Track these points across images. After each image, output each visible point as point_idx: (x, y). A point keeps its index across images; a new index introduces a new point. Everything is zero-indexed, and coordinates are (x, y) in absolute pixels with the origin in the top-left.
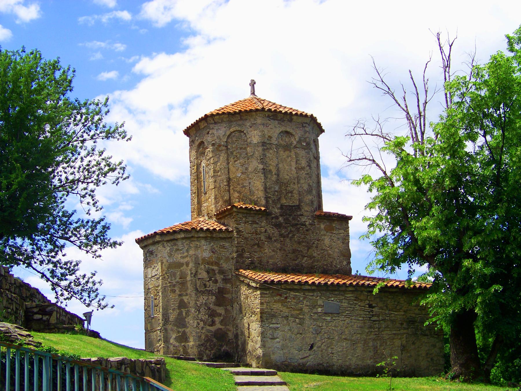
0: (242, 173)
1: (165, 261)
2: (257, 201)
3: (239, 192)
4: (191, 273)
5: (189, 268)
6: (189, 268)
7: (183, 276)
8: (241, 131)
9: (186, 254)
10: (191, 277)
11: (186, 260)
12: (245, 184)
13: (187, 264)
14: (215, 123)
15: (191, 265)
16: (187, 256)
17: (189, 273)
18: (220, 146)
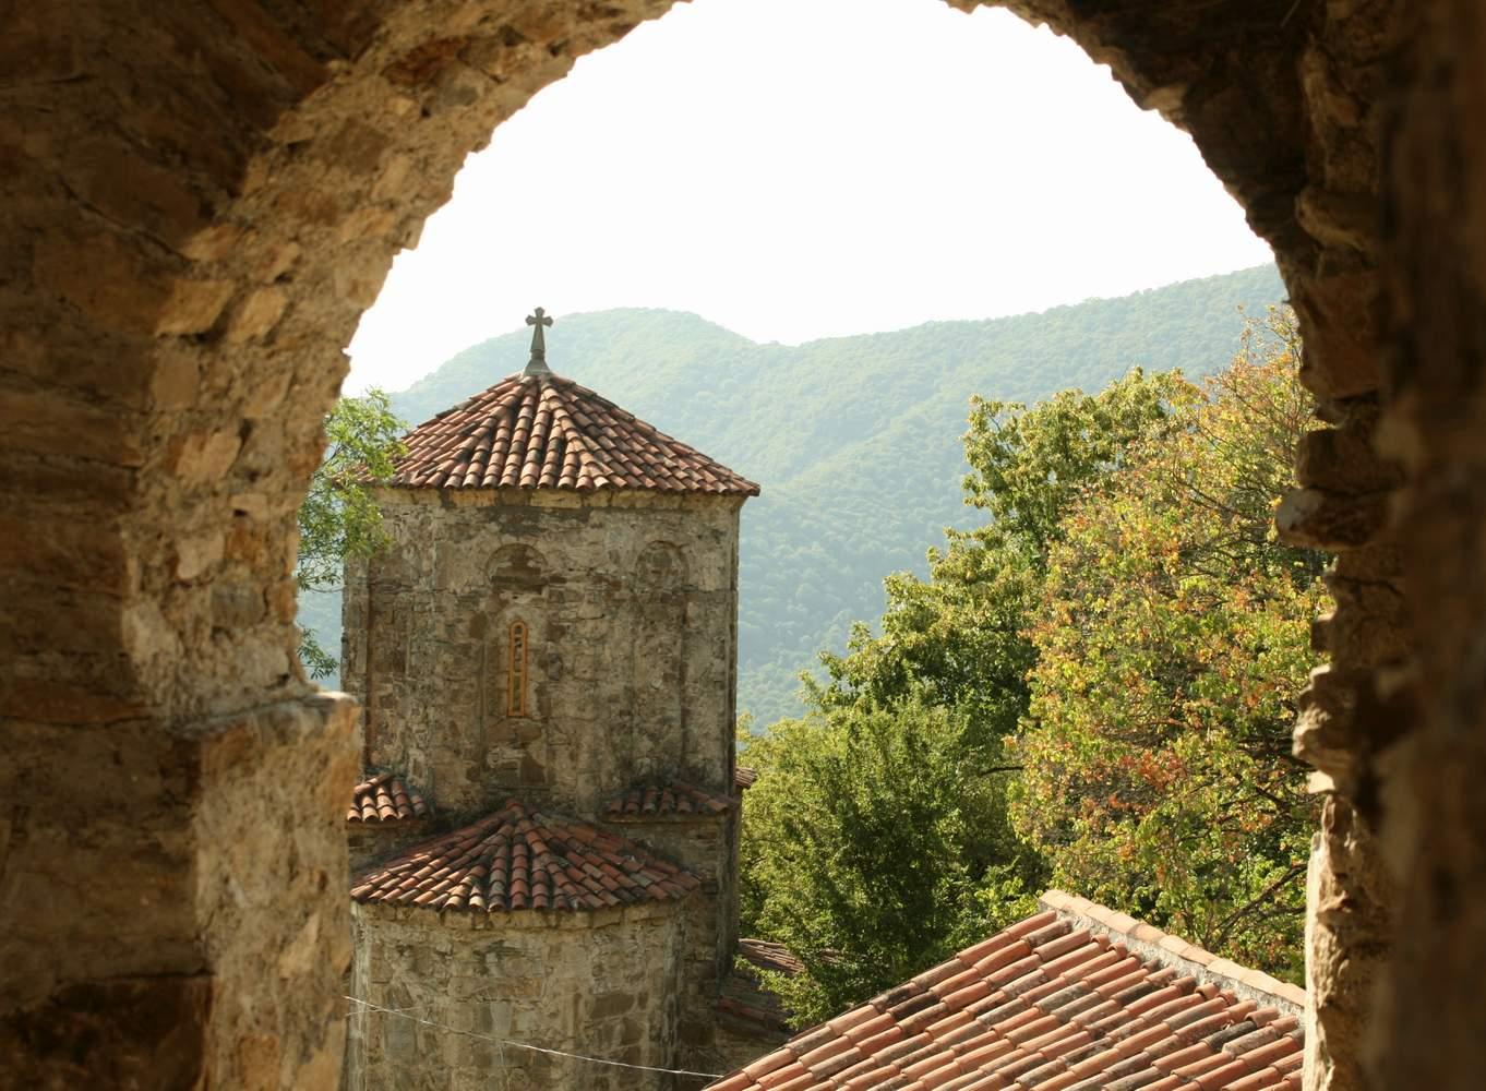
0: (666, 678)
1: (583, 990)
2: (704, 768)
3: (652, 737)
4: (652, 1028)
5: (648, 1010)
6: (648, 1010)
7: (630, 1035)
8: (672, 545)
9: (638, 969)
10: (652, 1039)
11: (643, 985)
12: (670, 714)
13: (643, 1000)
14: (609, 509)
15: (653, 1001)
16: (643, 974)
17: (647, 1025)
18: (616, 585)
